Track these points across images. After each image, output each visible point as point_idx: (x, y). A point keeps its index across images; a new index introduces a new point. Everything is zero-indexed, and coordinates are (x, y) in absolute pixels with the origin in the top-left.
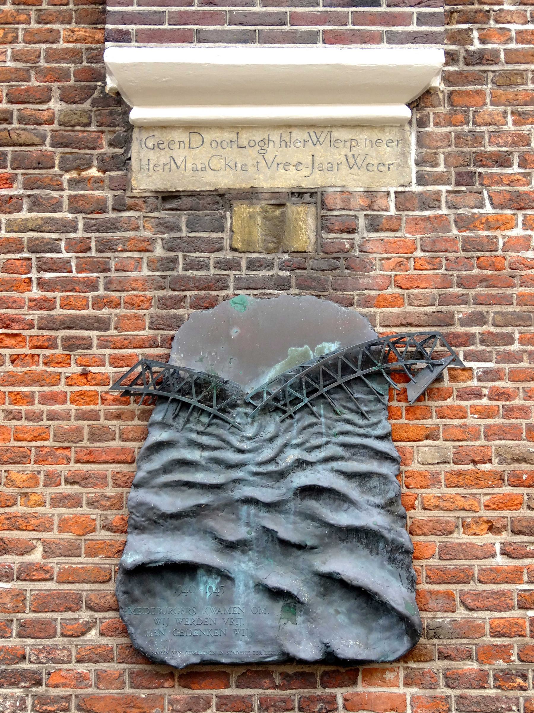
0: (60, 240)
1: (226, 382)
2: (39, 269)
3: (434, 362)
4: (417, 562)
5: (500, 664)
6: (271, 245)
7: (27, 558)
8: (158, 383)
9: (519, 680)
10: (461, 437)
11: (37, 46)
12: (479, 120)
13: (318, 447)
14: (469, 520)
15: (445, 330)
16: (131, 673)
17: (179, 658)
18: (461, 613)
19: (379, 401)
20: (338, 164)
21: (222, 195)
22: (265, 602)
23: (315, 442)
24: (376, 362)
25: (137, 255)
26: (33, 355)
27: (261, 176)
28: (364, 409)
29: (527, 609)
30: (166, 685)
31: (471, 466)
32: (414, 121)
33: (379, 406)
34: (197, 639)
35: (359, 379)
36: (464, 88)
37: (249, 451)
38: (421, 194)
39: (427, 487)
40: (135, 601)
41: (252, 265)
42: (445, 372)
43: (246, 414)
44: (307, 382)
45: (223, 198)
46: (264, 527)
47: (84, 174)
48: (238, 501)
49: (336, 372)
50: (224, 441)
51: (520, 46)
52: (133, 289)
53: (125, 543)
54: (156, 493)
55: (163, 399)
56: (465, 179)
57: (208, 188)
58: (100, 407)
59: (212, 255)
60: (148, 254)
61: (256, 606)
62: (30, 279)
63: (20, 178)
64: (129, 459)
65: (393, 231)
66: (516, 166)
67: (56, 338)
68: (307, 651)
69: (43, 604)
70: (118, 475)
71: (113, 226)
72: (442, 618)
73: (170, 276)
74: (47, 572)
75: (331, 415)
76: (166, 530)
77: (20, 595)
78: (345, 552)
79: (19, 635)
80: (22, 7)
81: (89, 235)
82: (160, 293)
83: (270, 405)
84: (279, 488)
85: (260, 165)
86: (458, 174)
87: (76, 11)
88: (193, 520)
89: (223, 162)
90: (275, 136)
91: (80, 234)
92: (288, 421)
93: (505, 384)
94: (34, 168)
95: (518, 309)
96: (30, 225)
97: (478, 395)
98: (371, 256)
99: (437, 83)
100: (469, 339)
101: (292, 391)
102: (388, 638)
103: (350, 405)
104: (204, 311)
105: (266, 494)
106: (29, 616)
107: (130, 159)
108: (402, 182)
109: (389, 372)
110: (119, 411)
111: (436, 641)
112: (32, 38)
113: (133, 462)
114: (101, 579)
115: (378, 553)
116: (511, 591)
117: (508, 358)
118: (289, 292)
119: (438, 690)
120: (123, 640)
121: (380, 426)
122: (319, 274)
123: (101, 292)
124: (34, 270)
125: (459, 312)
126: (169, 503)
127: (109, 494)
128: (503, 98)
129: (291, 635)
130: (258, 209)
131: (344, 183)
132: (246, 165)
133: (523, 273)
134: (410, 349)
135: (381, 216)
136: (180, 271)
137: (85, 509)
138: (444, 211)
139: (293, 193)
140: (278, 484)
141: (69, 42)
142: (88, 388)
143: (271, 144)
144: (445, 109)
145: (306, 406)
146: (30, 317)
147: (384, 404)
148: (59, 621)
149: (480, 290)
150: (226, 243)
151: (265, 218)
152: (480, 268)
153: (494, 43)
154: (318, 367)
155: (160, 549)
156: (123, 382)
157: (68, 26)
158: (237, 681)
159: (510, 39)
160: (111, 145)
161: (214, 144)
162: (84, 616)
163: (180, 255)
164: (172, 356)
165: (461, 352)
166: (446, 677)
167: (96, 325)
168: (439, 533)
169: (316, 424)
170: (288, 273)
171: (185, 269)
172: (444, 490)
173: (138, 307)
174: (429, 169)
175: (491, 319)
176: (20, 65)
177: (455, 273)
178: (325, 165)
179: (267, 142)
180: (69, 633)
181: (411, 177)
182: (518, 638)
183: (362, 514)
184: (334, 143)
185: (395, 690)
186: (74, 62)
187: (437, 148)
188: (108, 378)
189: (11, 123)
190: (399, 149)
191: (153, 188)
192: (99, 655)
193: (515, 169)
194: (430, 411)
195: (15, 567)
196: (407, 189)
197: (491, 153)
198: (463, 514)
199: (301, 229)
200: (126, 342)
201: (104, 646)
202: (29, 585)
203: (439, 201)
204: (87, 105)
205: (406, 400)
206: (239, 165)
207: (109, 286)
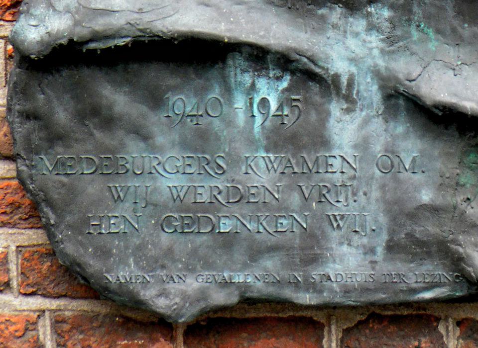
22: (412, 145)
34: (228, 241)
40: (55, 137)
61: (391, 151)
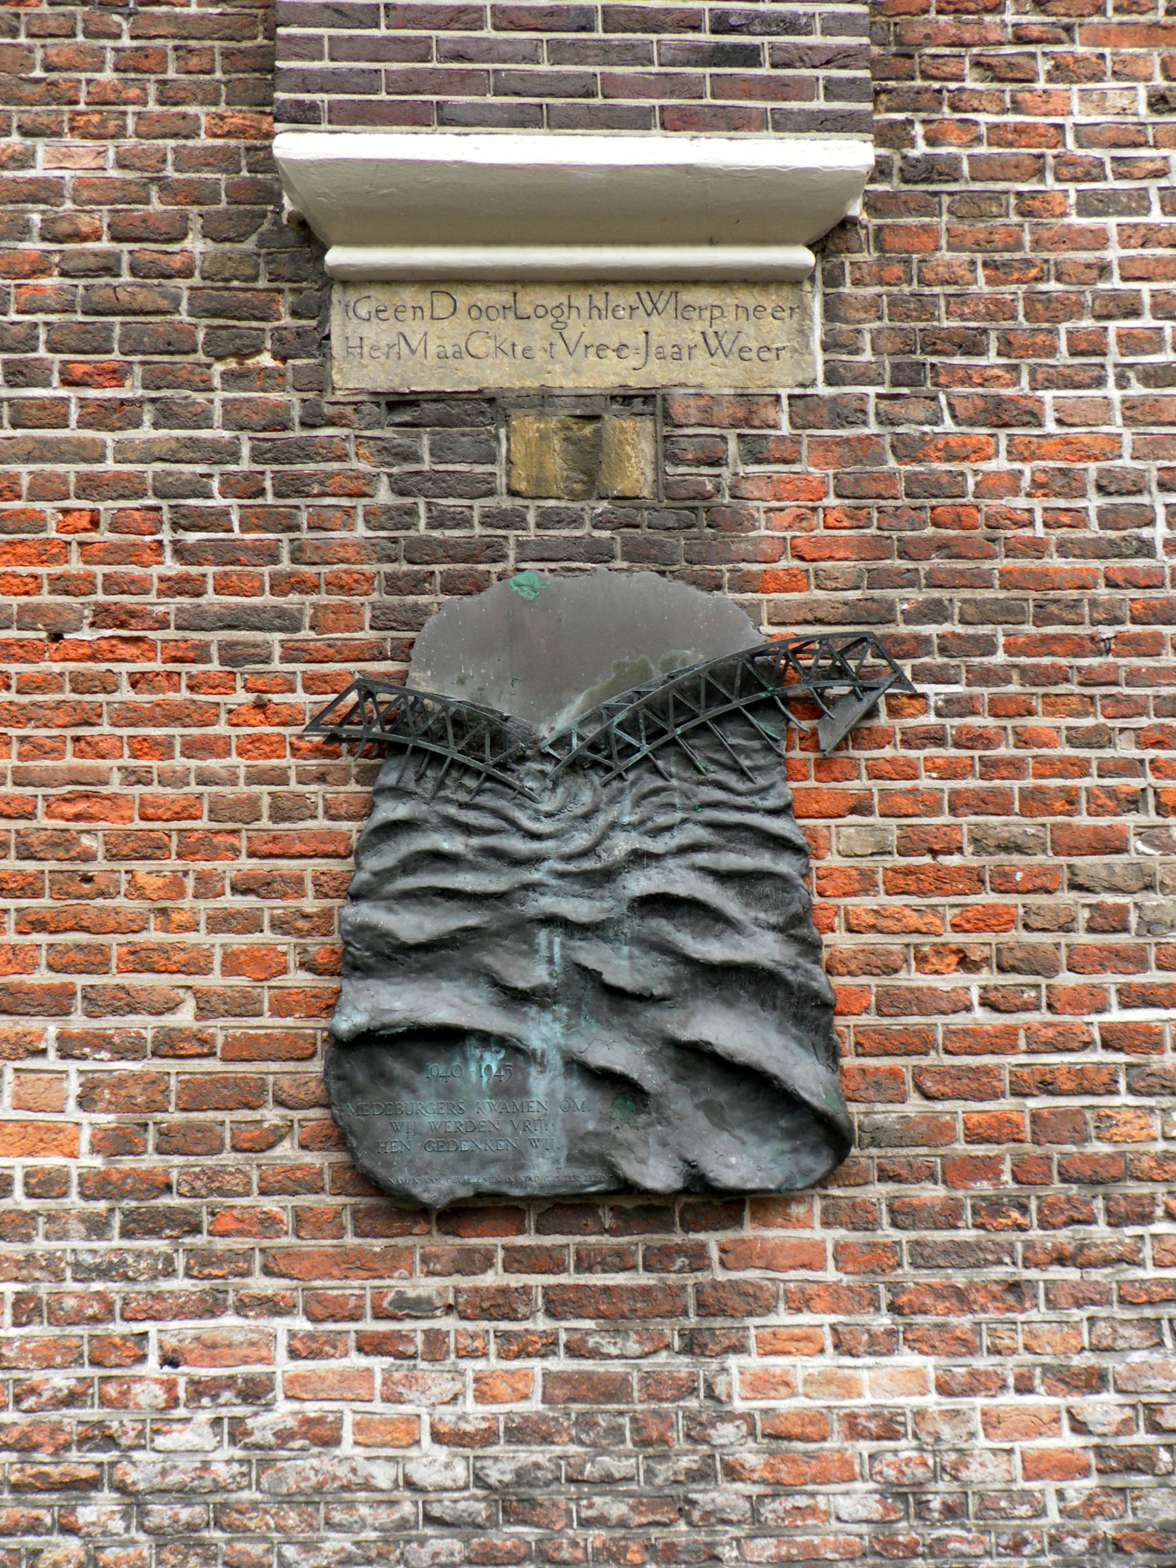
0: (210, 476)
1: (506, 719)
3: (863, 685)
4: (839, 1021)
5: (984, 1187)
6: (578, 487)
7: (168, 1020)
8: (388, 722)
9: (1015, 1214)
11: (160, 142)
12: (930, 275)
13: (669, 828)
14: (926, 949)
15: (879, 630)
16: (355, 1212)
17: (436, 1189)
18: (914, 1105)
19: (769, 749)
21: (491, 401)
22: (582, 1094)
23: (662, 820)
25: (345, 502)
26: (169, 674)
27: (558, 368)
28: (745, 763)
29: (1025, 1095)
30: (416, 1230)
31: (927, 859)
33: (771, 759)
34: (466, 1156)
35: (736, 714)
36: (902, 221)
38: (834, 399)
39: (854, 894)
40: (356, 1091)
41: (547, 520)
43: (543, 774)
44: (646, 718)
45: (489, 405)
46: (578, 965)
47: (250, 362)
48: (531, 920)
49: (697, 698)
50: (506, 819)
51: (996, 150)
52: (341, 561)
53: (338, 993)
54: (390, 910)
55: (397, 749)
58: (289, 761)
59: (477, 503)
60: (365, 501)
61: (569, 1098)
62: (160, 542)
63: (138, 370)
64: (342, 850)
65: (786, 462)
66: (993, 353)
67: (207, 645)
68: (658, 1175)
69: (196, 1096)
71: (305, 451)
72: (887, 1114)
74: (203, 1042)
75: (690, 774)
76: (406, 974)
77: (156, 1082)
79: (159, 1150)
80: (132, 75)
81: (260, 468)
82: (387, 568)
83: (585, 758)
84: (602, 898)
86: (895, 367)
87: (226, 83)
88: (456, 954)
89: (491, 343)
90: (580, 299)
91: (245, 465)
92: (616, 784)
93: (983, 721)
94: (161, 353)
95: (1002, 595)
96: (156, 451)
97: (936, 738)
98: (750, 504)
99: (856, 209)
100: (921, 644)
101: (620, 733)
102: (795, 1151)
103: (722, 757)
105: (579, 909)
106: (175, 1117)
107: (328, 337)
108: (800, 379)
109: (786, 701)
111: (874, 1151)
112: (150, 129)
115: (775, 1008)
116: (1000, 1067)
117: (985, 676)
120: (338, 1157)
121: (773, 792)
122: (660, 536)
123: (285, 565)
124: (166, 527)
126: (412, 925)
127: (308, 910)
128: (969, 241)
129: (628, 1147)
130: (553, 423)
131: (700, 380)
132: (529, 348)
133: (1009, 533)
134: (822, 662)
135: (765, 437)
137: (268, 936)
138: (873, 428)
139: (613, 398)
140: (600, 892)
141: (215, 136)
143: (574, 312)
144: (868, 256)
145: (646, 758)
146: (162, 609)
148: (228, 1125)
149: (937, 562)
150: (501, 482)
151: (566, 439)
152: (936, 524)
154: (665, 692)
155: (398, 1005)
156: (327, 718)
157: (213, 109)
158: (537, 1222)
159: (978, 139)
160: (295, 314)
162: (272, 1116)
163: (421, 503)
164: (412, 674)
165: (907, 667)
166: (892, 1211)
167: (277, 622)
169: (664, 789)
170: (606, 534)
172: (884, 899)
174: (845, 357)
177: (895, 535)
178: (668, 350)
180: (246, 1145)
182: (1012, 1145)
183: (745, 942)
184: (684, 312)
185: (805, 1234)
186: (226, 171)
189: (118, 275)
190: (793, 323)
191: (370, 387)
193: (992, 358)
194: (856, 767)
195: (149, 1035)
196: (809, 391)
198: (916, 939)
199: (629, 458)
200: (331, 651)
201: (310, 1166)
202: (172, 1066)
203: (864, 412)
204: (250, 245)
205: (817, 748)
206: (519, 349)
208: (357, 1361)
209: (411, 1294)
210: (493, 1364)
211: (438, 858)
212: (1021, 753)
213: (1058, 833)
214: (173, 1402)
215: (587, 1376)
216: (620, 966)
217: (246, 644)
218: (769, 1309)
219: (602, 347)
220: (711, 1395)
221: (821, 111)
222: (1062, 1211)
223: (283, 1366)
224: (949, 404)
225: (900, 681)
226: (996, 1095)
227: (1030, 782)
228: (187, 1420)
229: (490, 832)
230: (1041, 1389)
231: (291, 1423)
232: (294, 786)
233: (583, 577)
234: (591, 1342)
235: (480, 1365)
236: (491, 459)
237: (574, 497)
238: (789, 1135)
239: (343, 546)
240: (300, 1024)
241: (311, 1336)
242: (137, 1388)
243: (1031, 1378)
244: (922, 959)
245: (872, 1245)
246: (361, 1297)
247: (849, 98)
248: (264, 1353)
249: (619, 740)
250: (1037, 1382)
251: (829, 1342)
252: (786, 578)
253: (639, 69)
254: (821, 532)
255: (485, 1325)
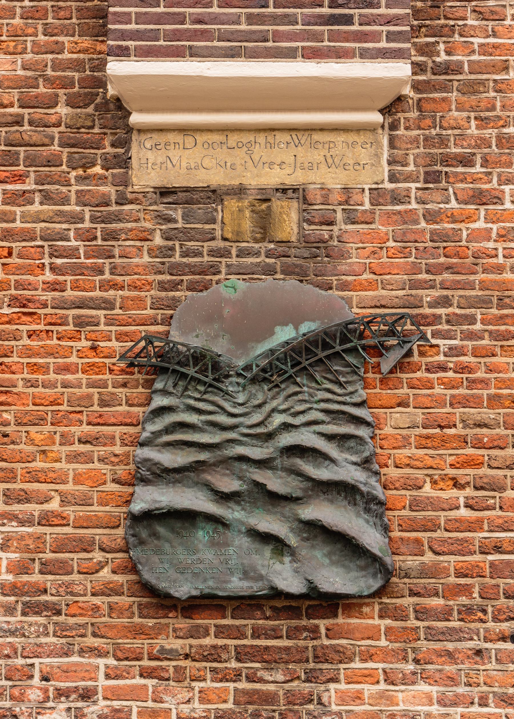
0: (69, 230)
2: (51, 255)
5: (464, 600)
6: (258, 236)
7: (46, 507)
8: (159, 357)
9: (480, 614)
10: (429, 405)
11: (44, 56)
12: (445, 124)
13: (303, 412)
14: (436, 477)
16: (140, 605)
18: (429, 557)
19: (356, 373)
20: (318, 164)
21: (214, 191)
24: (352, 338)
25: (138, 243)
26: (47, 331)
27: (249, 174)
28: (342, 379)
29: (487, 553)
30: (170, 615)
31: (438, 430)
32: (386, 125)
33: (355, 377)
35: (337, 354)
36: (431, 96)
37: (240, 415)
38: (393, 191)
39: (399, 448)
42: (415, 347)
43: (238, 384)
45: (214, 195)
46: (254, 481)
47: (89, 171)
48: (231, 458)
51: (483, 58)
52: (136, 274)
53: (132, 494)
54: (159, 451)
56: (432, 177)
57: (201, 185)
58: (108, 376)
59: (206, 244)
61: (248, 549)
62: (43, 264)
63: (32, 175)
65: (367, 223)
66: (478, 166)
67: (67, 316)
70: (125, 436)
71: (118, 218)
73: (168, 262)
74: (64, 518)
75: (314, 385)
76: (167, 484)
77: (39, 538)
78: (326, 503)
79: (41, 572)
80: (30, 21)
81: (95, 226)
84: (267, 447)
85: (247, 164)
86: (426, 173)
87: (78, 25)
88: (192, 474)
90: (261, 138)
91: (87, 224)
92: (276, 390)
94: (45, 166)
95: (480, 293)
96: (42, 217)
97: (443, 368)
98: (348, 245)
99: (407, 91)
100: (436, 319)
104: (200, 294)
105: (256, 452)
106: (49, 556)
107: (130, 158)
108: (375, 180)
109: (364, 348)
110: (126, 380)
111: (406, 580)
113: (138, 425)
114: (112, 524)
115: (355, 504)
116: (473, 538)
118: (275, 277)
119: (409, 622)
123: (107, 276)
124: (46, 256)
125: (427, 296)
126: (170, 459)
127: (117, 452)
128: (467, 106)
130: (246, 203)
131: (323, 181)
132: (234, 164)
133: (485, 261)
135: (356, 210)
136: (177, 258)
137: (97, 465)
138: (414, 205)
139: (277, 190)
140: (266, 444)
141: (73, 53)
142: (97, 360)
143: (258, 145)
144: (414, 114)
145: (291, 376)
146: (44, 298)
147: (359, 375)
148: (75, 560)
149: (447, 276)
150: (218, 233)
151: (252, 211)
152: (446, 256)
153: (459, 55)
156: (128, 355)
157: (72, 39)
158: (232, 613)
159: (473, 52)
160: (113, 145)
161: (206, 146)
162: (98, 556)
163: (177, 244)
164: (172, 333)
165: (429, 331)
166: (416, 611)
167: (103, 305)
168: (409, 488)
169: (300, 392)
171: (182, 256)
172: (414, 451)
173: (140, 289)
174: (400, 168)
175: (456, 302)
176: (29, 73)
177: (424, 262)
178: (306, 165)
179: (253, 144)
180: (85, 570)
181: (383, 176)
182: (479, 579)
184: (314, 145)
185: (370, 622)
186: (78, 71)
187: (407, 149)
188: (115, 351)
189: (23, 126)
190: (372, 151)
191: (153, 184)
192: (111, 589)
195: (36, 514)
196: (380, 186)
197: (456, 155)
198: (430, 472)
199: (285, 221)
200: (130, 320)
202: (48, 530)
203: (409, 197)
204: (90, 110)
205: (380, 373)
206: (228, 164)
207: (114, 270)
208: (139, 681)
209: (168, 647)
210: (209, 684)
211: (183, 426)
212: (488, 376)
213: (507, 418)
214: (47, 699)
215: (256, 692)
216: (275, 483)
217: (87, 316)
218: (351, 660)
219: (272, 163)
220: (320, 703)
221: (384, 48)
222: (504, 613)
223: (102, 682)
224: (454, 193)
225: (423, 337)
226: (472, 553)
227: (493, 391)
228: (54, 708)
229: (210, 413)
230: (492, 705)
231: (106, 711)
232: (110, 389)
233: (259, 283)
234: (259, 674)
235: (202, 684)
236: (213, 221)
237: (256, 241)
238: (362, 568)
239: (137, 266)
240: (113, 509)
241: (116, 667)
242: (29, 691)
243: (487, 699)
244: (434, 483)
245: (405, 628)
246: (142, 648)
247: (399, 41)
248: (93, 675)
249: (277, 367)
250: (490, 701)
251: (382, 678)
252: (366, 284)
253: (291, 27)
254: (385, 260)
255: (204, 664)
